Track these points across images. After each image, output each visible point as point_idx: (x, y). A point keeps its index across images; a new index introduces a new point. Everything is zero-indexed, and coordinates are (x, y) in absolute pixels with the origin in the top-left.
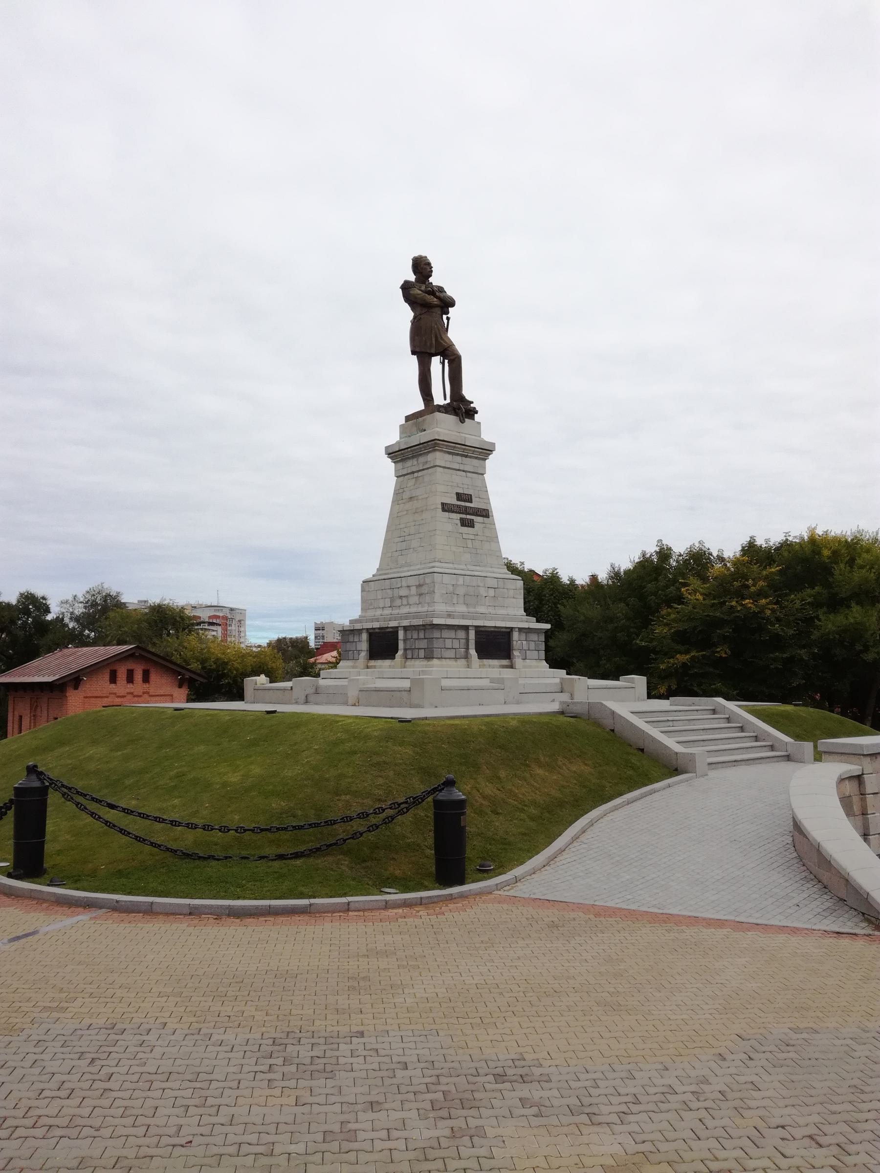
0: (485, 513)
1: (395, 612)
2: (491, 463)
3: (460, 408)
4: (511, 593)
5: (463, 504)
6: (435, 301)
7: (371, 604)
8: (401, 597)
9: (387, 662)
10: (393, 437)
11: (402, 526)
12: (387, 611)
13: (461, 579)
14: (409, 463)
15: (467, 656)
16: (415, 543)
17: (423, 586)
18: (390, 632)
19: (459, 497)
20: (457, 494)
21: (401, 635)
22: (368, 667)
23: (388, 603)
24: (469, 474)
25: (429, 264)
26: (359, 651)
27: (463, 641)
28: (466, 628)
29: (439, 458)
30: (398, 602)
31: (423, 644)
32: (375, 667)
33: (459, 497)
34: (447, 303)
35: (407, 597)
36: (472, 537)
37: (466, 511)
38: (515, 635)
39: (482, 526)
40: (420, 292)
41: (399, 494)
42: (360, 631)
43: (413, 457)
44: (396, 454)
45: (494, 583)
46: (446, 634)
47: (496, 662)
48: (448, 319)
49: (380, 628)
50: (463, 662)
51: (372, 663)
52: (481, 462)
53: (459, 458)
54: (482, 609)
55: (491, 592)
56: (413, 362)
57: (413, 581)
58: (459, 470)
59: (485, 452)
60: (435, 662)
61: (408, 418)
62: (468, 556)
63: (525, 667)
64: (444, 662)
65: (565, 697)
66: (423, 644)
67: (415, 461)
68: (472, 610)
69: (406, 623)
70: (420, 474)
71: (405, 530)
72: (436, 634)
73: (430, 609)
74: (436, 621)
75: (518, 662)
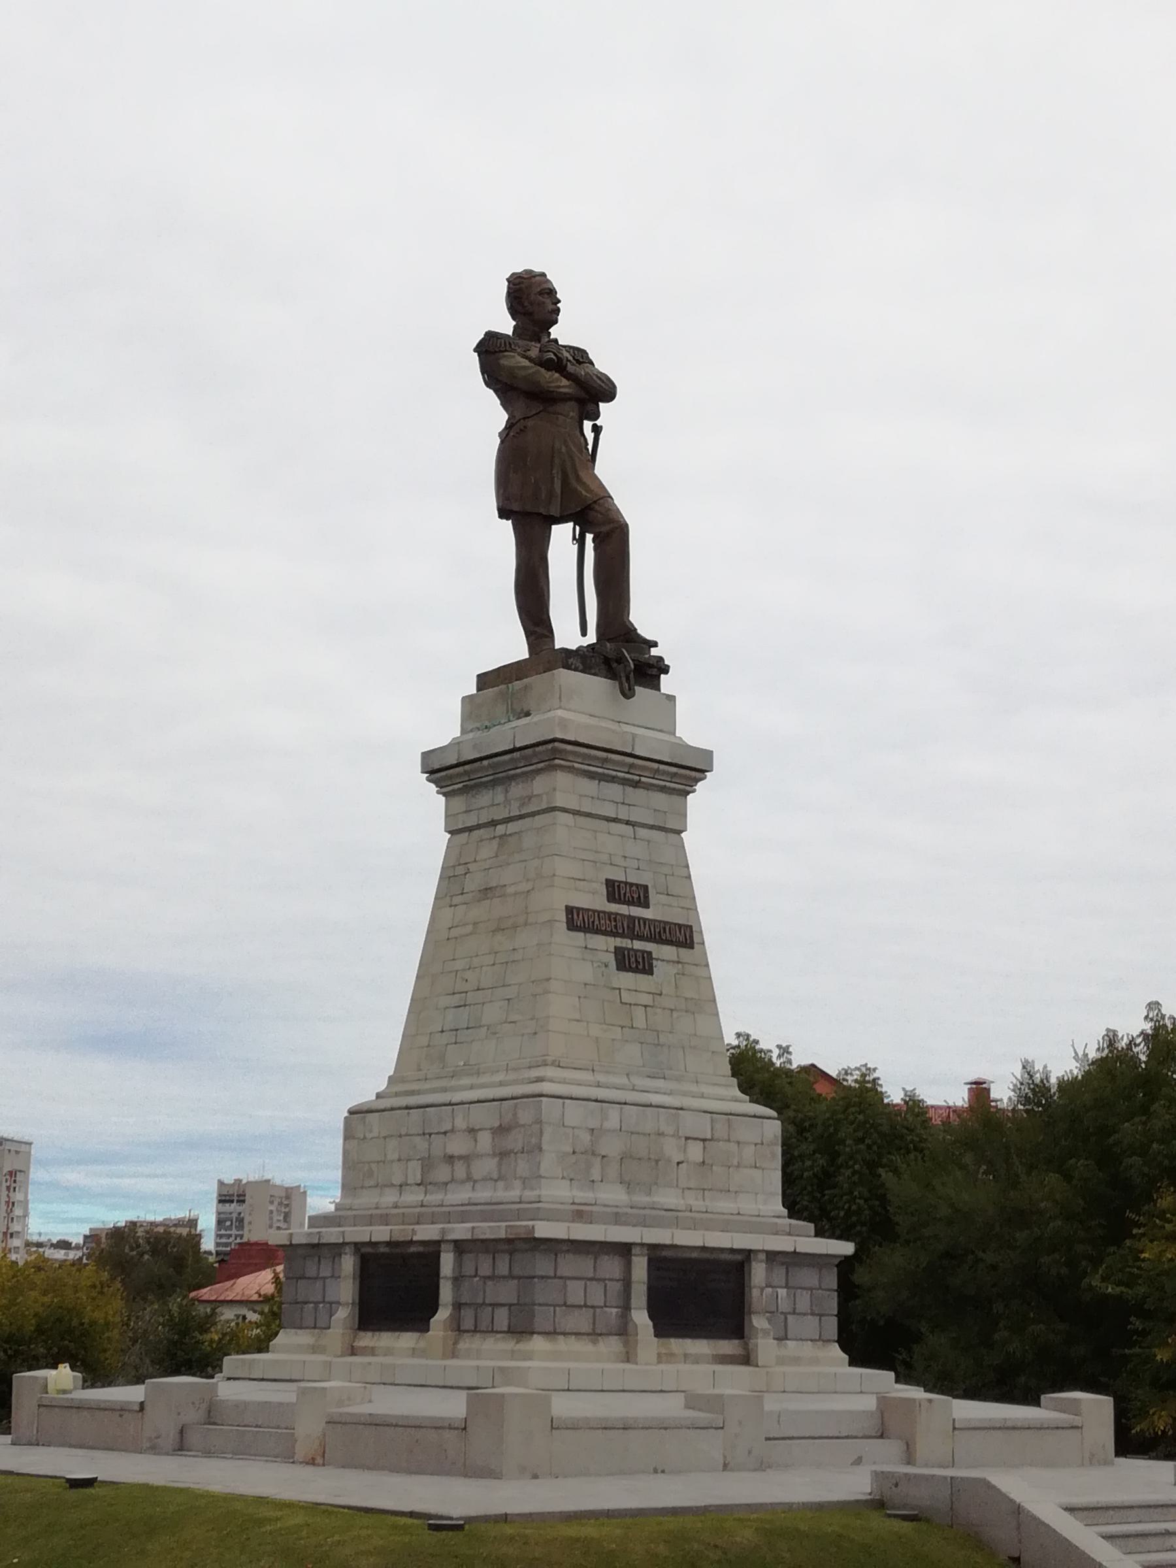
0: (684, 936)
1: (435, 1197)
2: (699, 801)
3: (620, 660)
4: (749, 1152)
5: (623, 909)
6: (564, 385)
7: (370, 1174)
8: (450, 1159)
9: (407, 1340)
10: (444, 728)
11: (459, 965)
12: (413, 1197)
14: (484, 798)
15: (624, 1330)
16: (492, 1013)
17: (513, 1133)
18: (413, 1255)
19: (615, 890)
20: (610, 884)
21: (447, 1262)
22: (353, 1351)
23: (415, 1172)
24: (643, 833)
25: (551, 292)
26: (332, 1307)
27: (618, 1286)
28: (624, 1250)
29: (565, 788)
30: (442, 1173)
31: (507, 1292)
32: (372, 1351)
33: (615, 890)
34: (595, 392)
35: (466, 1158)
36: (646, 999)
38: (758, 1273)
39: (672, 970)
40: (526, 363)
41: (453, 880)
42: (336, 1250)
43: (494, 783)
44: (448, 772)
45: (703, 1127)
46: (570, 1265)
47: (701, 1347)
48: (597, 430)
49: (388, 1244)
50: (613, 1344)
51: (367, 1339)
52: (676, 799)
53: (614, 791)
54: (668, 1198)
55: (695, 1152)
56: (502, 537)
57: (484, 1117)
58: (615, 820)
59: (687, 771)
60: (538, 1343)
61: (484, 681)
63: (781, 1361)
64: (562, 1344)
65: (886, 1457)
66: (507, 1292)
67: (499, 795)
68: (642, 1199)
69: (460, 1231)
70: (512, 827)
71: (468, 975)
72: (542, 1265)
73: (529, 1194)
74: (544, 1230)
75: (765, 1346)
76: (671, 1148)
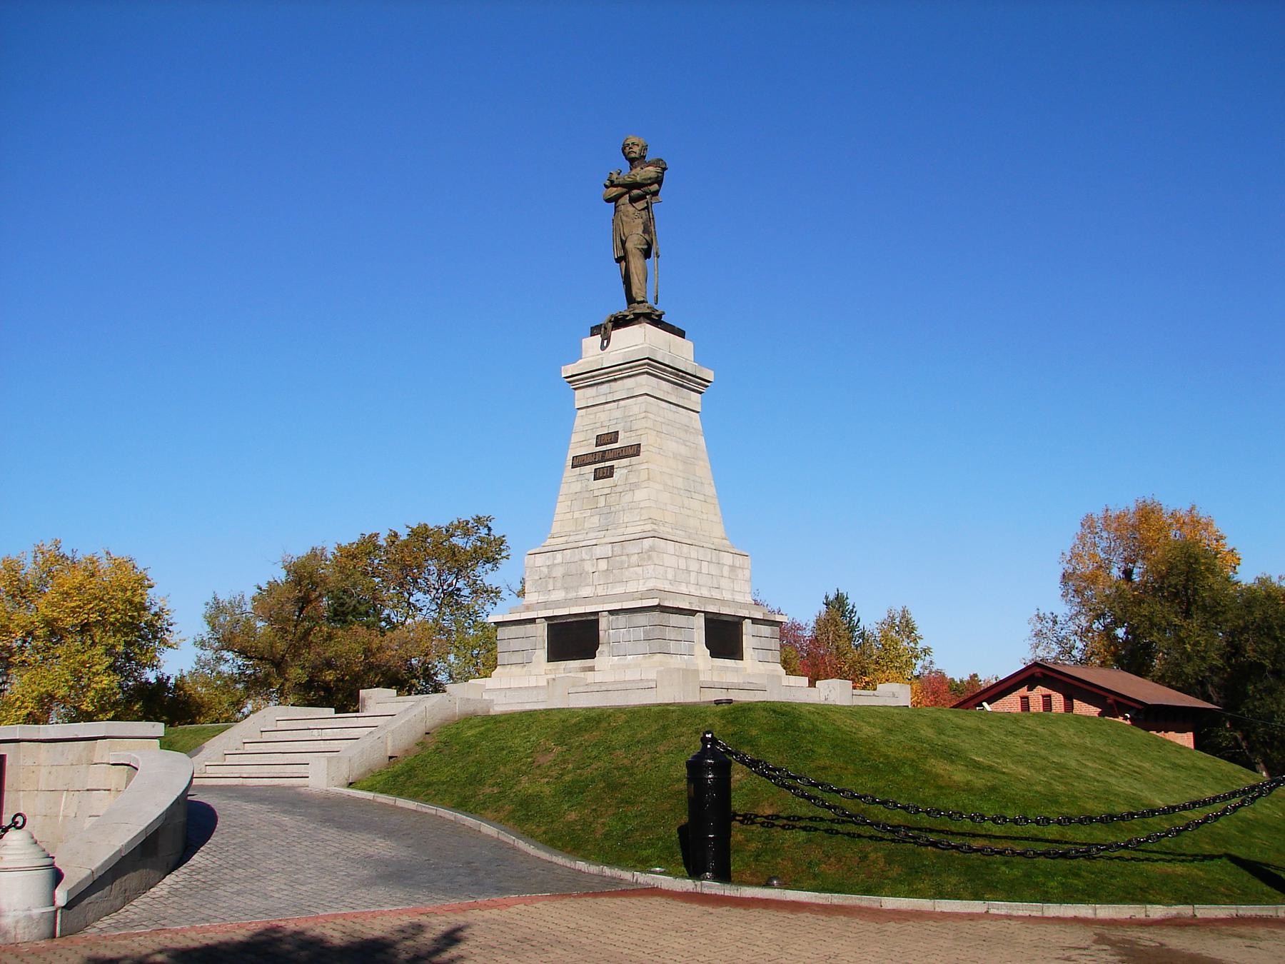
4: (634, 559)
13: (559, 555)
28: (533, 621)
33: (600, 440)
36: (607, 491)
37: (603, 457)
45: (607, 551)
55: (603, 565)
62: (595, 520)
68: (572, 595)
76: (589, 567)
